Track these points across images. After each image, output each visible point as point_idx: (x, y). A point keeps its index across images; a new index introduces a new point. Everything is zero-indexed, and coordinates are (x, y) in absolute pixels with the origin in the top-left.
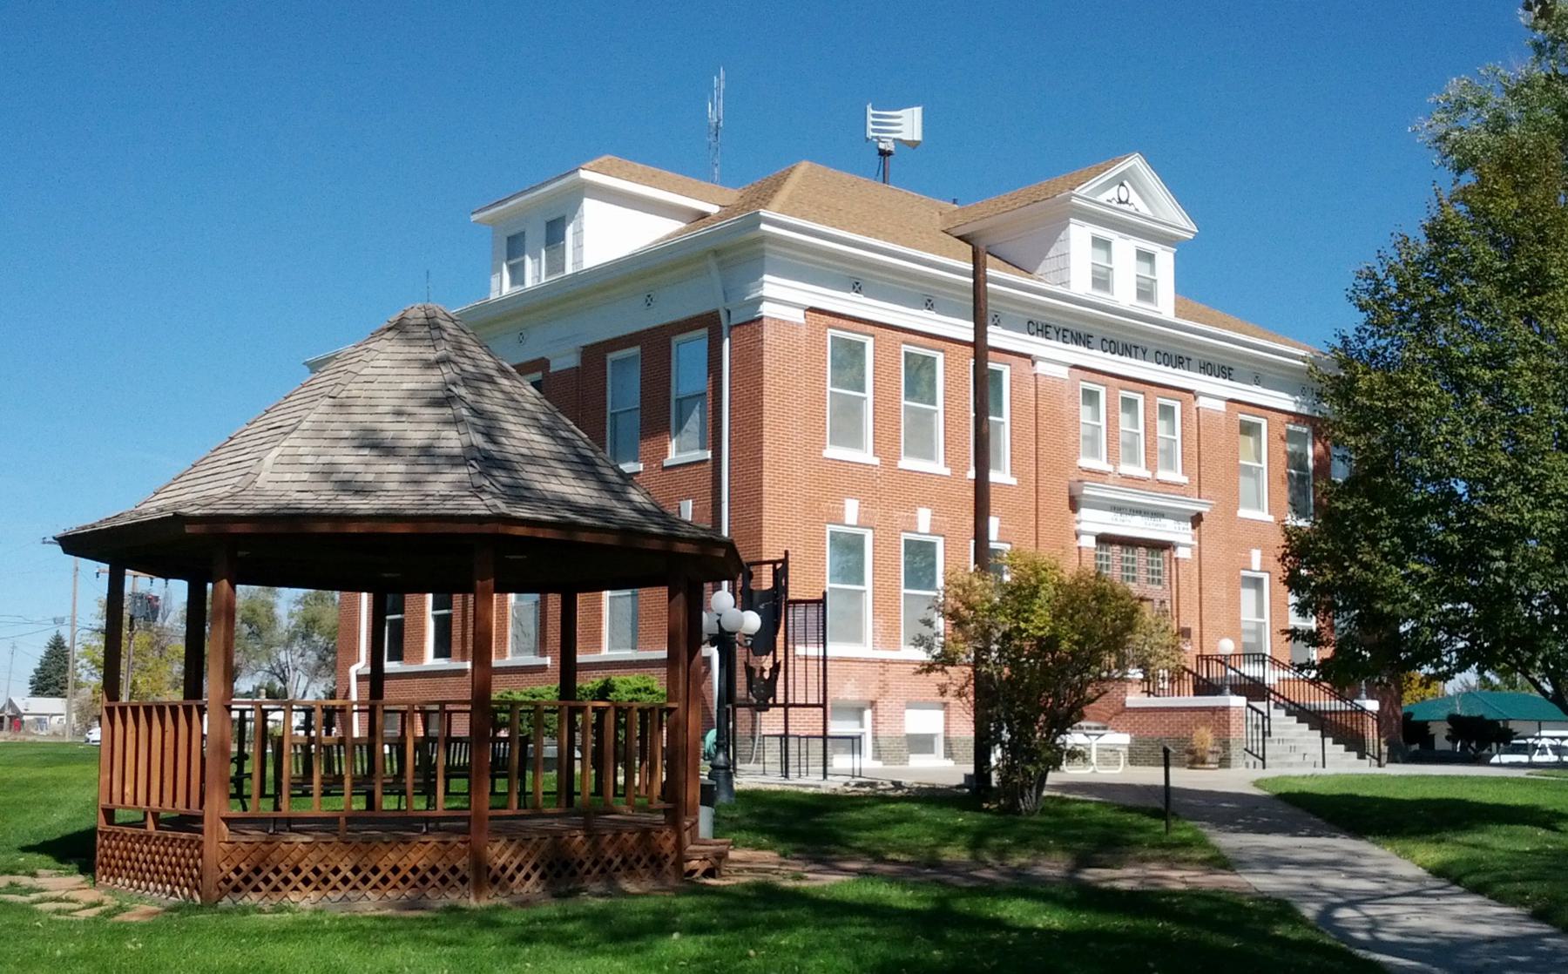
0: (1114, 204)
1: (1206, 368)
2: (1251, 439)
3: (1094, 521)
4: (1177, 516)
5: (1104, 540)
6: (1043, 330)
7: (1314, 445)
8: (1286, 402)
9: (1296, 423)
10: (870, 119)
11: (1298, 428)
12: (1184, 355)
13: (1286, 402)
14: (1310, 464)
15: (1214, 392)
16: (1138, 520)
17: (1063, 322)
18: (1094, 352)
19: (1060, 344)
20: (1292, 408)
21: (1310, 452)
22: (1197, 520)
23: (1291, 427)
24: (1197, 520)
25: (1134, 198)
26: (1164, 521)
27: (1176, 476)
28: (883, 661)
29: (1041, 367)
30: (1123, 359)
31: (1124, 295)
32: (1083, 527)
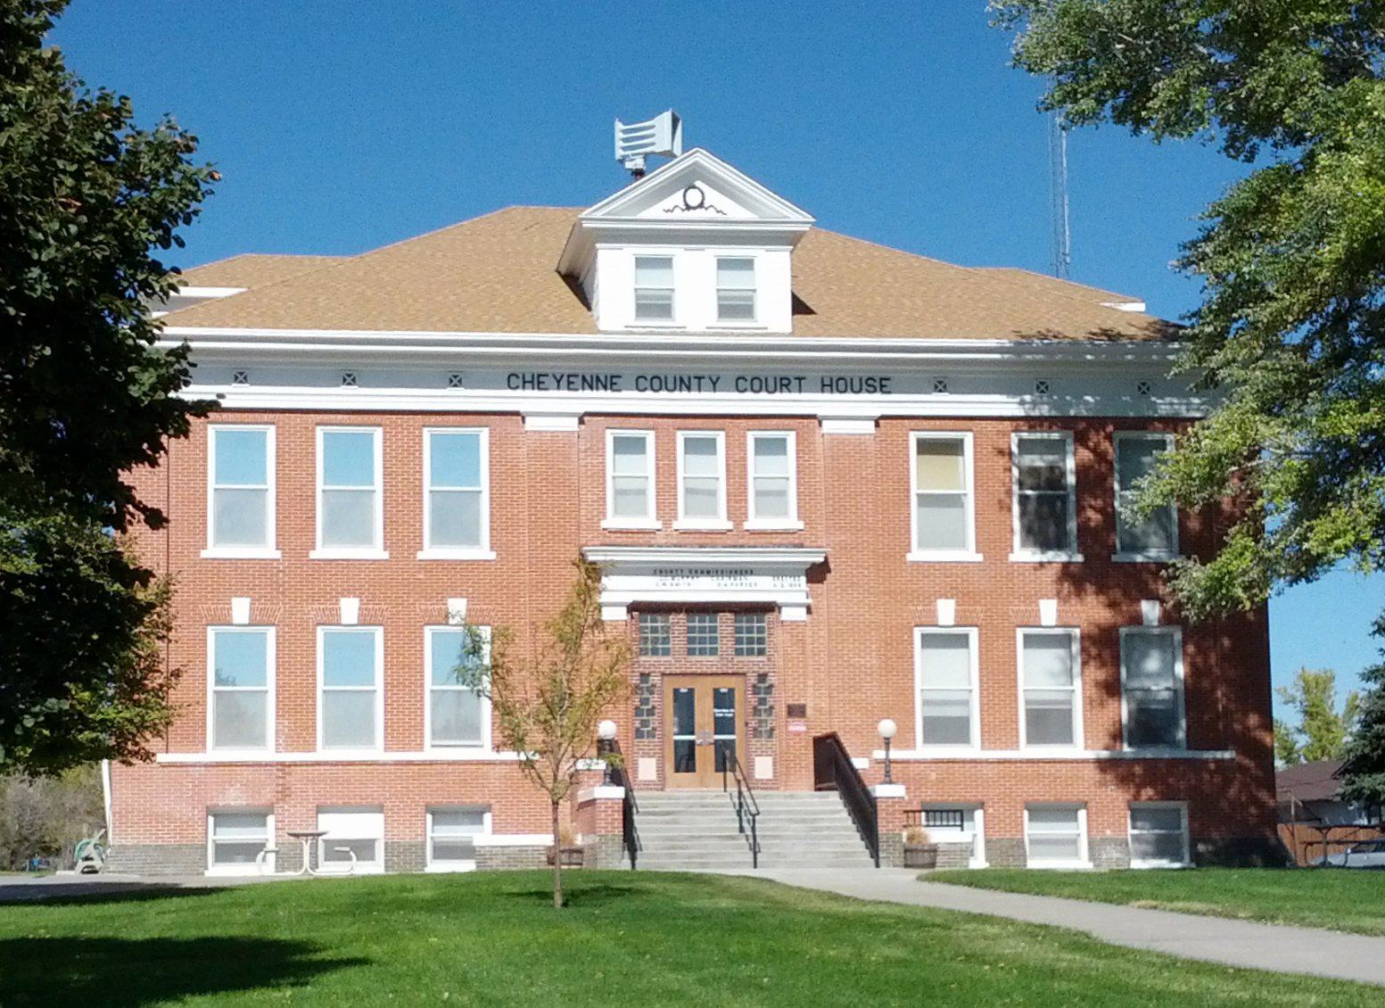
0: (678, 214)
1: (836, 382)
2: (960, 458)
3: (618, 592)
4: (777, 571)
5: (634, 608)
6: (537, 382)
7: (1075, 454)
8: (1008, 406)
9: (1031, 429)
10: (619, 135)
11: (1038, 436)
12: (791, 375)
13: (1008, 406)
14: (1071, 480)
15: (849, 415)
16: (683, 582)
17: (566, 368)
18: (625, 394)
19: (564, 393)
20: (1020, 412)
21: (1070, 464)
22: (816, 573)
23: (1025, 435)
24: (816, 573)
25: (713, 196)
26: (751, 579)
27: (792, 522)
28: (283, 764)
29: (531, 424)
30: (677, 394)
31: (695, 320)
32: (604, 598)
